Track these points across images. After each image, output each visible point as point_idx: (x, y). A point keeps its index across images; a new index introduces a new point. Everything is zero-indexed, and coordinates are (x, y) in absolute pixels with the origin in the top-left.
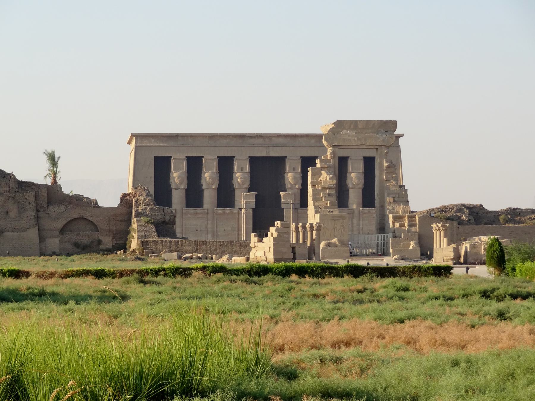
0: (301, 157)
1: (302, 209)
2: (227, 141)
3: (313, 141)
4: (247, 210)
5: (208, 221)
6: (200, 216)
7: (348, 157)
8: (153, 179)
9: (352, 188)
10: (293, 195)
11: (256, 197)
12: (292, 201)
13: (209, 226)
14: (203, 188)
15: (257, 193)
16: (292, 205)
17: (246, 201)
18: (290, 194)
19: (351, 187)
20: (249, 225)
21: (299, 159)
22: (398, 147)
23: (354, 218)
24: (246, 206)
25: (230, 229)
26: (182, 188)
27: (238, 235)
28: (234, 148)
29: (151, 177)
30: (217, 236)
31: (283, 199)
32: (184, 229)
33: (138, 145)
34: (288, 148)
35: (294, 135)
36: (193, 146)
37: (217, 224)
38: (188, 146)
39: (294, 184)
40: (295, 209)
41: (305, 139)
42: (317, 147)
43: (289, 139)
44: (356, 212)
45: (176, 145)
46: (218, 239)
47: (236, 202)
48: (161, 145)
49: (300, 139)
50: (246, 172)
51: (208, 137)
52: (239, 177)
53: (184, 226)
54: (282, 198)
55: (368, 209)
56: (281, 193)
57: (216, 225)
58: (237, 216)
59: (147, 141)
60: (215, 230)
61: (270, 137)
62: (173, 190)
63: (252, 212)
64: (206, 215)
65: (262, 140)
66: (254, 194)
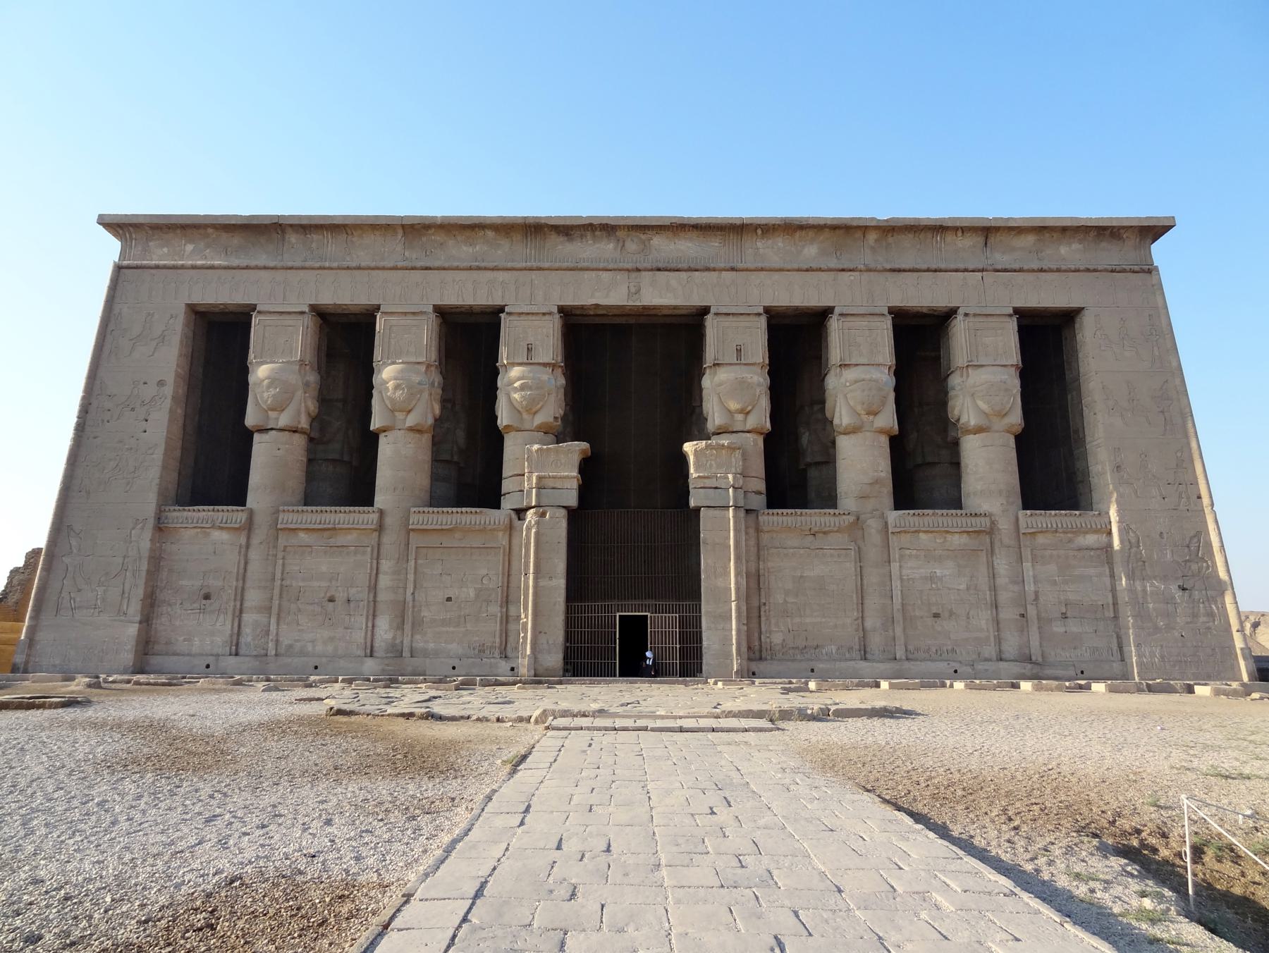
0: (768, 310)
1: (771, 511)
2: (477, 248)
3: (811, 251)
4: (543, 515)
5: (383, 562)
6: (350, 538)
7: (950, 313)
8: (168, 390)
9: (979, 430)
10: (738, 454)
11: (587, 467)
12: (734, 478)
13: (384, 581)
14: (372, 428)
15: (585, 445)
16: (734, 492)
17: (540, 478)
18: (723, 445)
19: (973, 423)
20: (551, 578)
21: (759, 314)
22: (1149, 272)
23: (997, 551)
24: (537, 495)
25: (472, 594)
26: (284, 420)
27: (506, 619)
28: (501, 276)
29: (161, 383)
30: (413, 624)
31: (696, 471)
32: (276, 591)
33: (125, 263)
34: (714, 274)
35: (738, 223)
36: (339, 268)
37: (415, 573)
38: (320, 268)
39: (741, 411)
40: (748, 511)
41: (780, 242)
42: (830, 270)
43: (717, 244)
44: (1004, 525)
45: (272, 264)
46: (418, 637)
47: (507, 485)
48: (217, 263)
49: (759, 244)
50: (545, 365)
51: (400, 232)
52: (517, 384)
53: (278, 583)
54: (692, 470)
55: (1053, 512)
56: (688, 447)
57: (411, 577)
58: (505, 542)
59: (165, 250)
60: (409, 597)
61: (643, 237)
62: (256, 437)
63: (563, 524)
64: (376, 534)
65: (611, 246)
66: (576, 449)
